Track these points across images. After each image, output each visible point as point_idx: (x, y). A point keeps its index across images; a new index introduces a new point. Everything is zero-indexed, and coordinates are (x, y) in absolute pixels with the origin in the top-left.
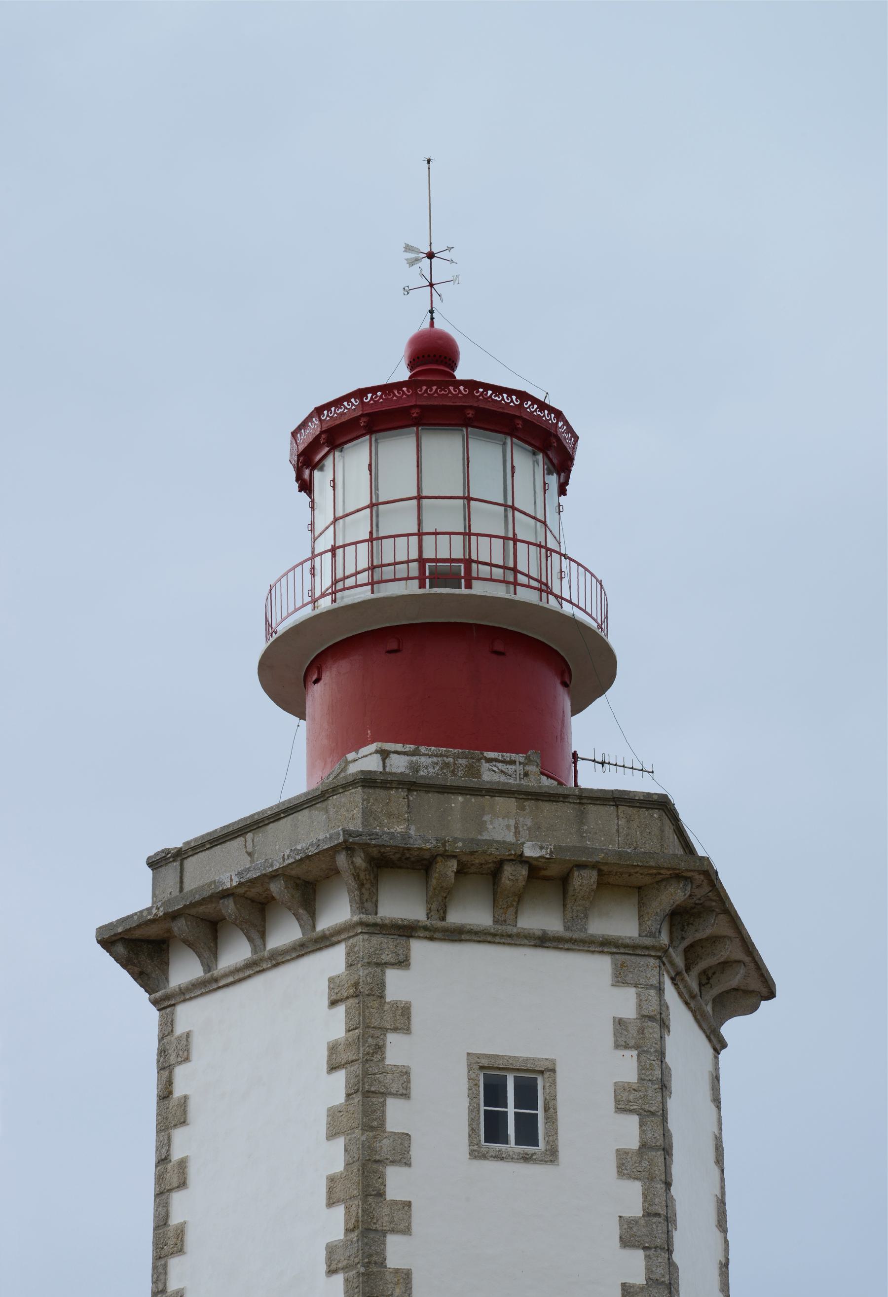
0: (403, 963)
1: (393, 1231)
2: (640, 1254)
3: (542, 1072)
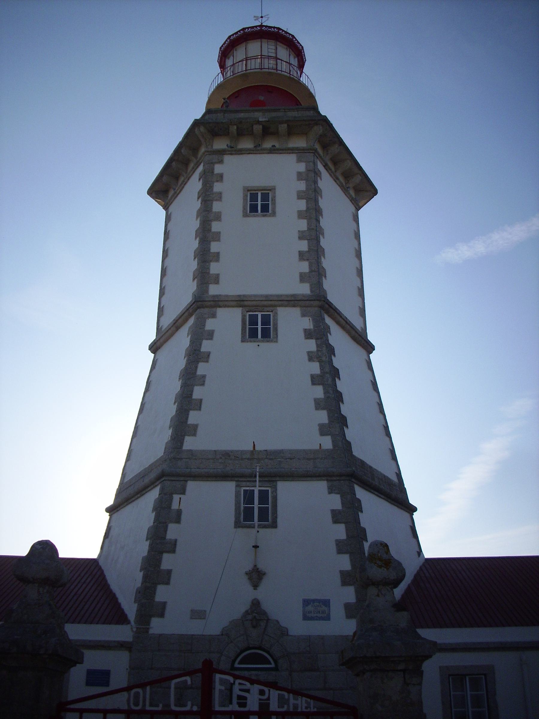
0: (221, 162)
1: (213, 241)
2: (306, 241)
3: (270, 190)
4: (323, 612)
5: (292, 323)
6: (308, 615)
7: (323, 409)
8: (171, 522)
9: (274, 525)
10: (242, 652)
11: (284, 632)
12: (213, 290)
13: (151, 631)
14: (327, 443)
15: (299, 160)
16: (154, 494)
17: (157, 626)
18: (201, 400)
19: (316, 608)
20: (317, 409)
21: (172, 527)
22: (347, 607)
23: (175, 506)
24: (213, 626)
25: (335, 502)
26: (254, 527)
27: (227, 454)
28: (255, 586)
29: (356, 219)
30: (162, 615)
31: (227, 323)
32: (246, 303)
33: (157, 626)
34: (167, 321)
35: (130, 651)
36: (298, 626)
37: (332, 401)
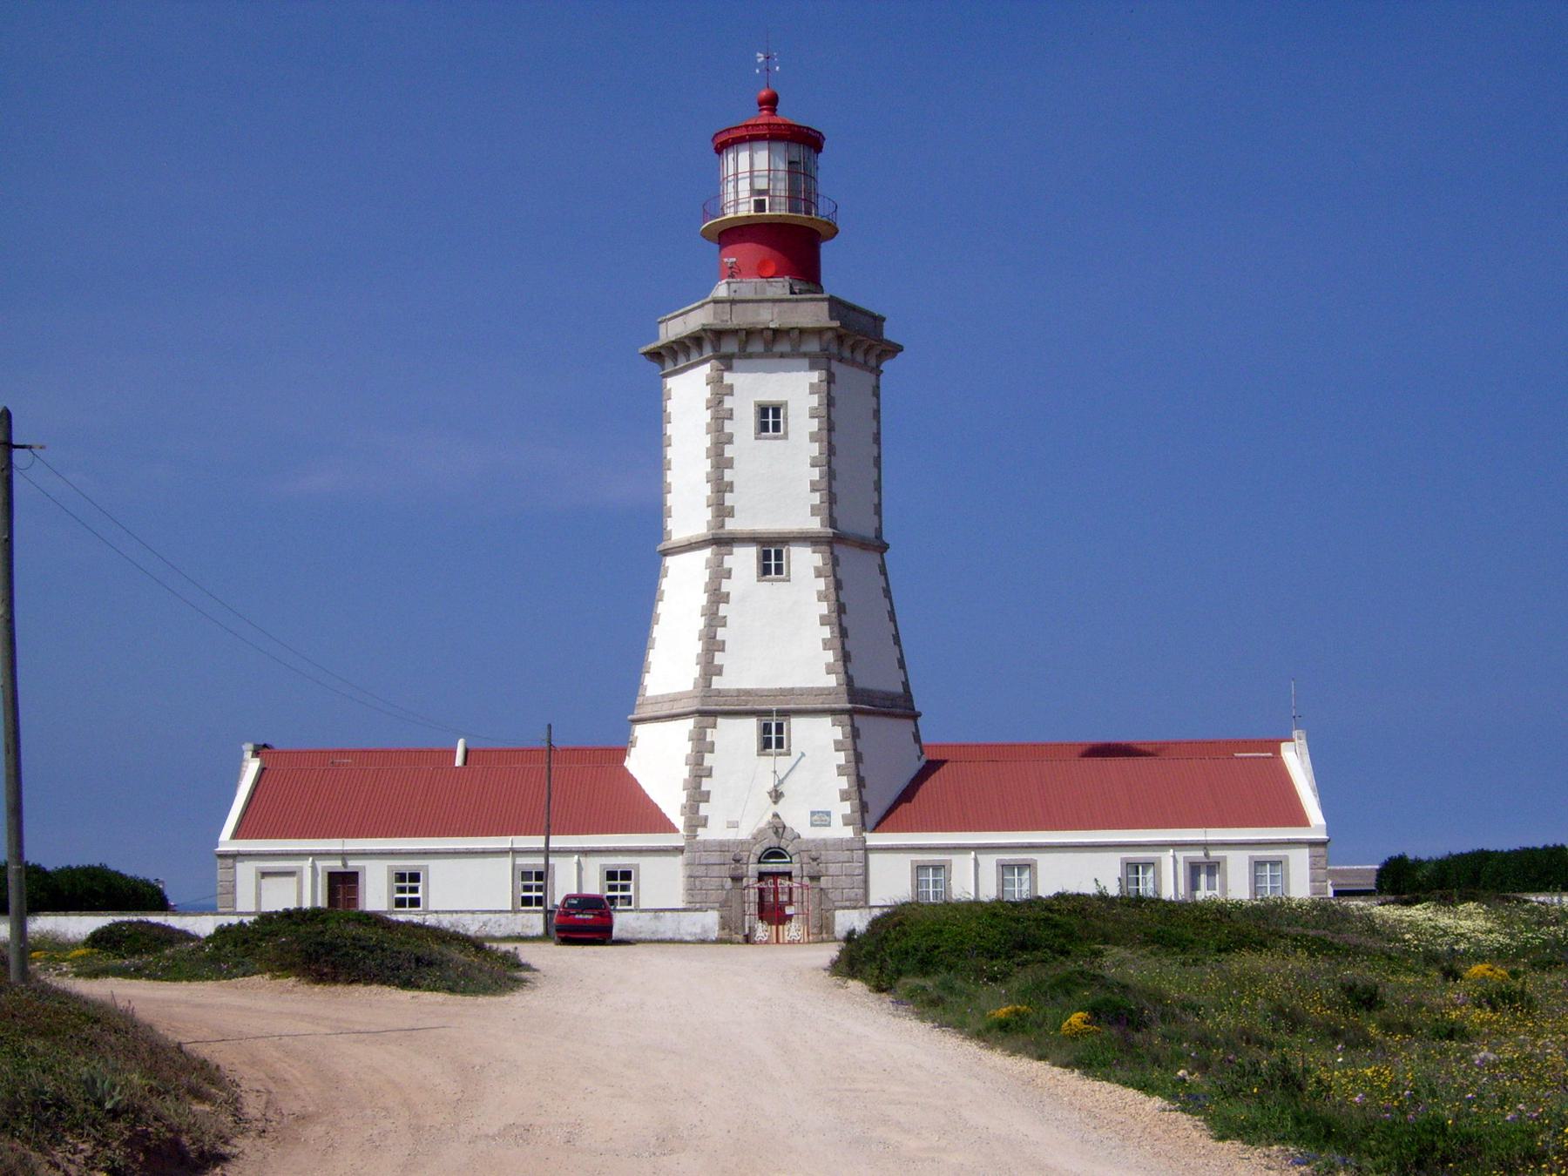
12: (731, 525)
17: (703, 834)
19: (820, 818)
21: (707, 756)
22: (844, 816)
24: (744, 833)
30: (705, 826)
31: (745, 559)
36: (808, 832)
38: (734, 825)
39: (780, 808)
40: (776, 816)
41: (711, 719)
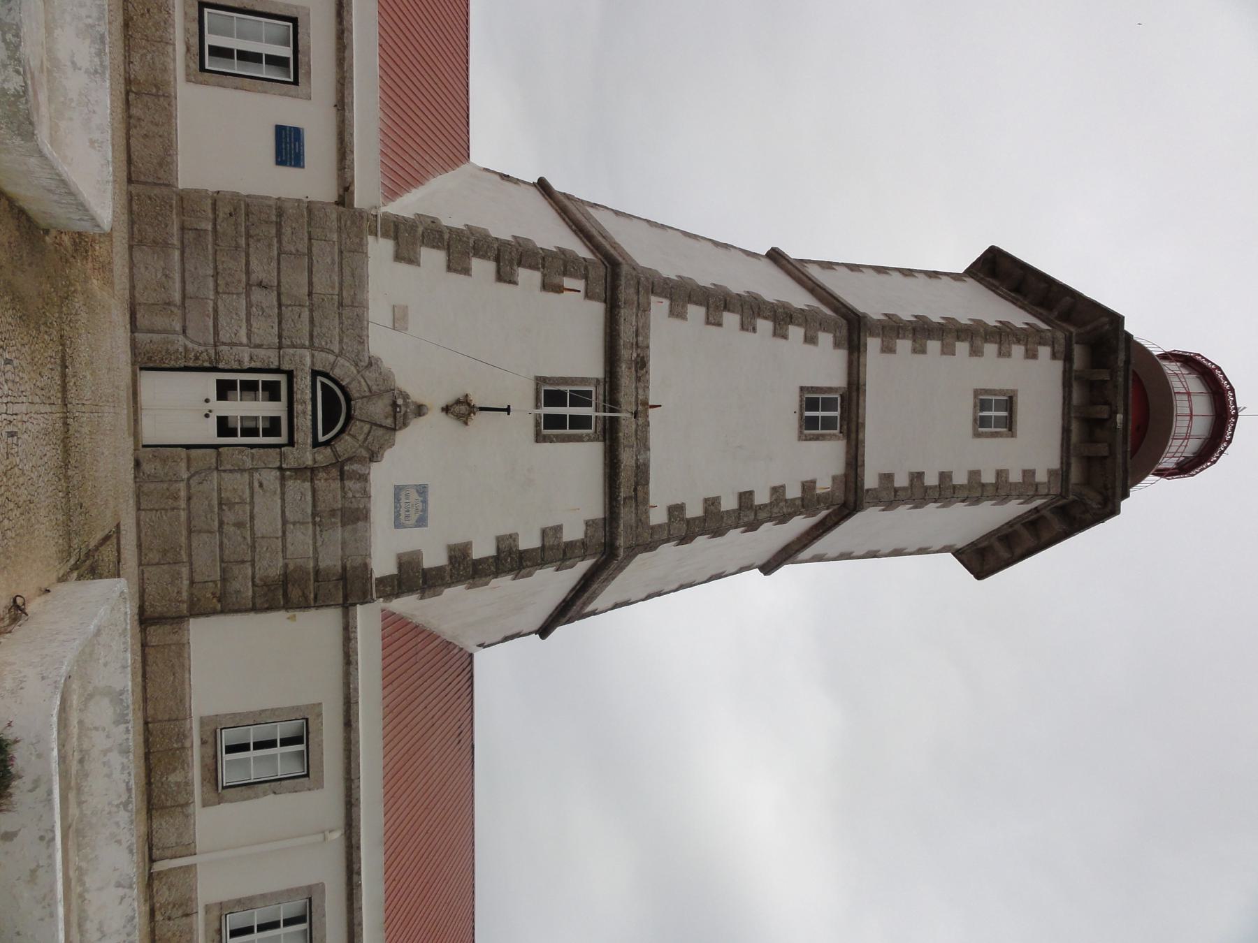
0: (1054, 356)
1: (943, 345)
2: (937, 483)
4: (407, 517)
5: (822, 462)
6: (403, 493)
7: (706, 511)
8: (544, 276)
9: (539, 438)
10: (342, 388)
11: (374, 457)
12: (873, 344)
13: (371, 239)
14: (658, 516)
15: (1051, 473)
16: (582, 252)
17: (379, 249)
18: (719, 324)
19: (413, 505)
20: (706, 500)
23: (568, 282)
24: (382, 342)
25: (573, 532)
26: (537, 407)
27: (641, 364)
28: (446, 409)
29: (944, 550)
30: (398, 257)
32: (854, 394)
33: (379, 249)
34: (814, 272)
35: (337, 203)
36: (384, 477)
37: (714, 521)
38: (399, 319)
39: (435, 417)
40: (420, 410)
41: (599, 289)
